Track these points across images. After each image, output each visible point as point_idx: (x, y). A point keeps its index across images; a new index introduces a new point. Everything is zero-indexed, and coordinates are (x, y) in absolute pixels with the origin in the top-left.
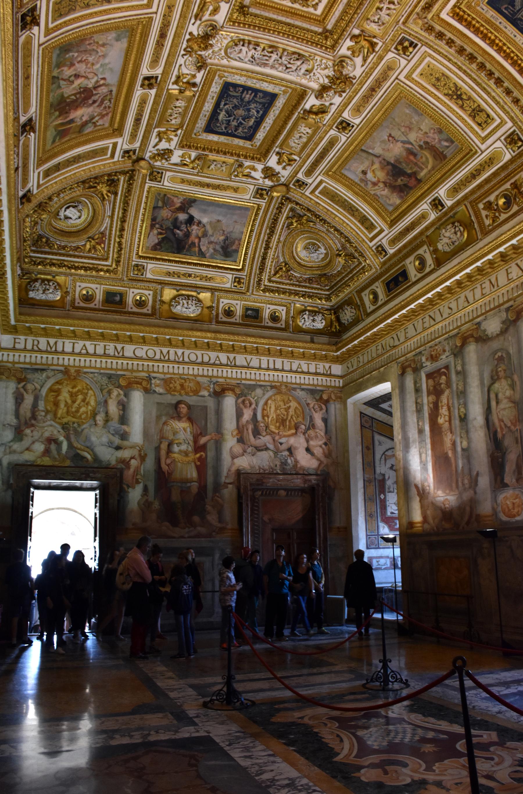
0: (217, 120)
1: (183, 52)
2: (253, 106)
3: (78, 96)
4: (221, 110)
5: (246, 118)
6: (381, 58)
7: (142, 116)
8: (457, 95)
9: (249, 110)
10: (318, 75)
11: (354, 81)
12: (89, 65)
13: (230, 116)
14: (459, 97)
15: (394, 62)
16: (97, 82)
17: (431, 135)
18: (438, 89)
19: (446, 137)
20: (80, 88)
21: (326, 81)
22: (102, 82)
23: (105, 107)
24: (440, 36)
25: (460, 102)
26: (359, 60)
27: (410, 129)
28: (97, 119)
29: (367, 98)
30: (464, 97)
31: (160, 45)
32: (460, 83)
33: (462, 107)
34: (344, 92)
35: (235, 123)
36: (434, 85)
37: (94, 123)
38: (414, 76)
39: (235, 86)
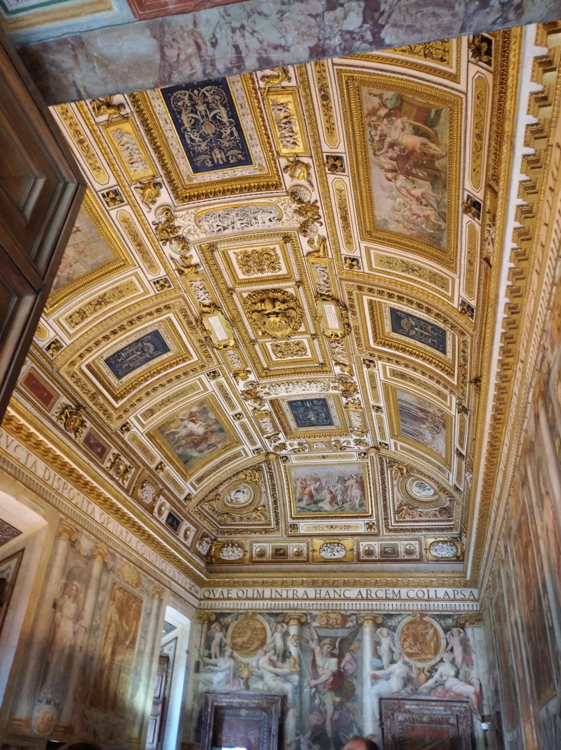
0: (225, 106)
1: (318, 204)
2: (204, 146)
3: (414, 171)
4: (231, 123)
5: (196, 125)
6: (165, 268)
7: (323, 106)
8: (101, 301)
9: (203, 137)
10: (187, 223)
11: (161, 243)
12: (408, 207)
13: (214, 117)
14: (99, 303)
15: (155, 272)
16: (395, 179)
17: (68, 270)
18: (113, 289)
19: (62, 283)
20: (413, 182)
21: (176, 224)
22: (390, 175)
23: (376, 129)
24: (158, 310)
25: (94, 303)
26: (177, 257)
27: (80, 253)
28: (383, 112)
29: (135, 236)
30: (98, 307)
31: (343, 208)
32: (110, 306)
33: (90, 304)
34: (156, 229)
35: (201, 108)
36: (117, 288)
37: (385, 105)
38: (134, 278)
39: (240, 163)
